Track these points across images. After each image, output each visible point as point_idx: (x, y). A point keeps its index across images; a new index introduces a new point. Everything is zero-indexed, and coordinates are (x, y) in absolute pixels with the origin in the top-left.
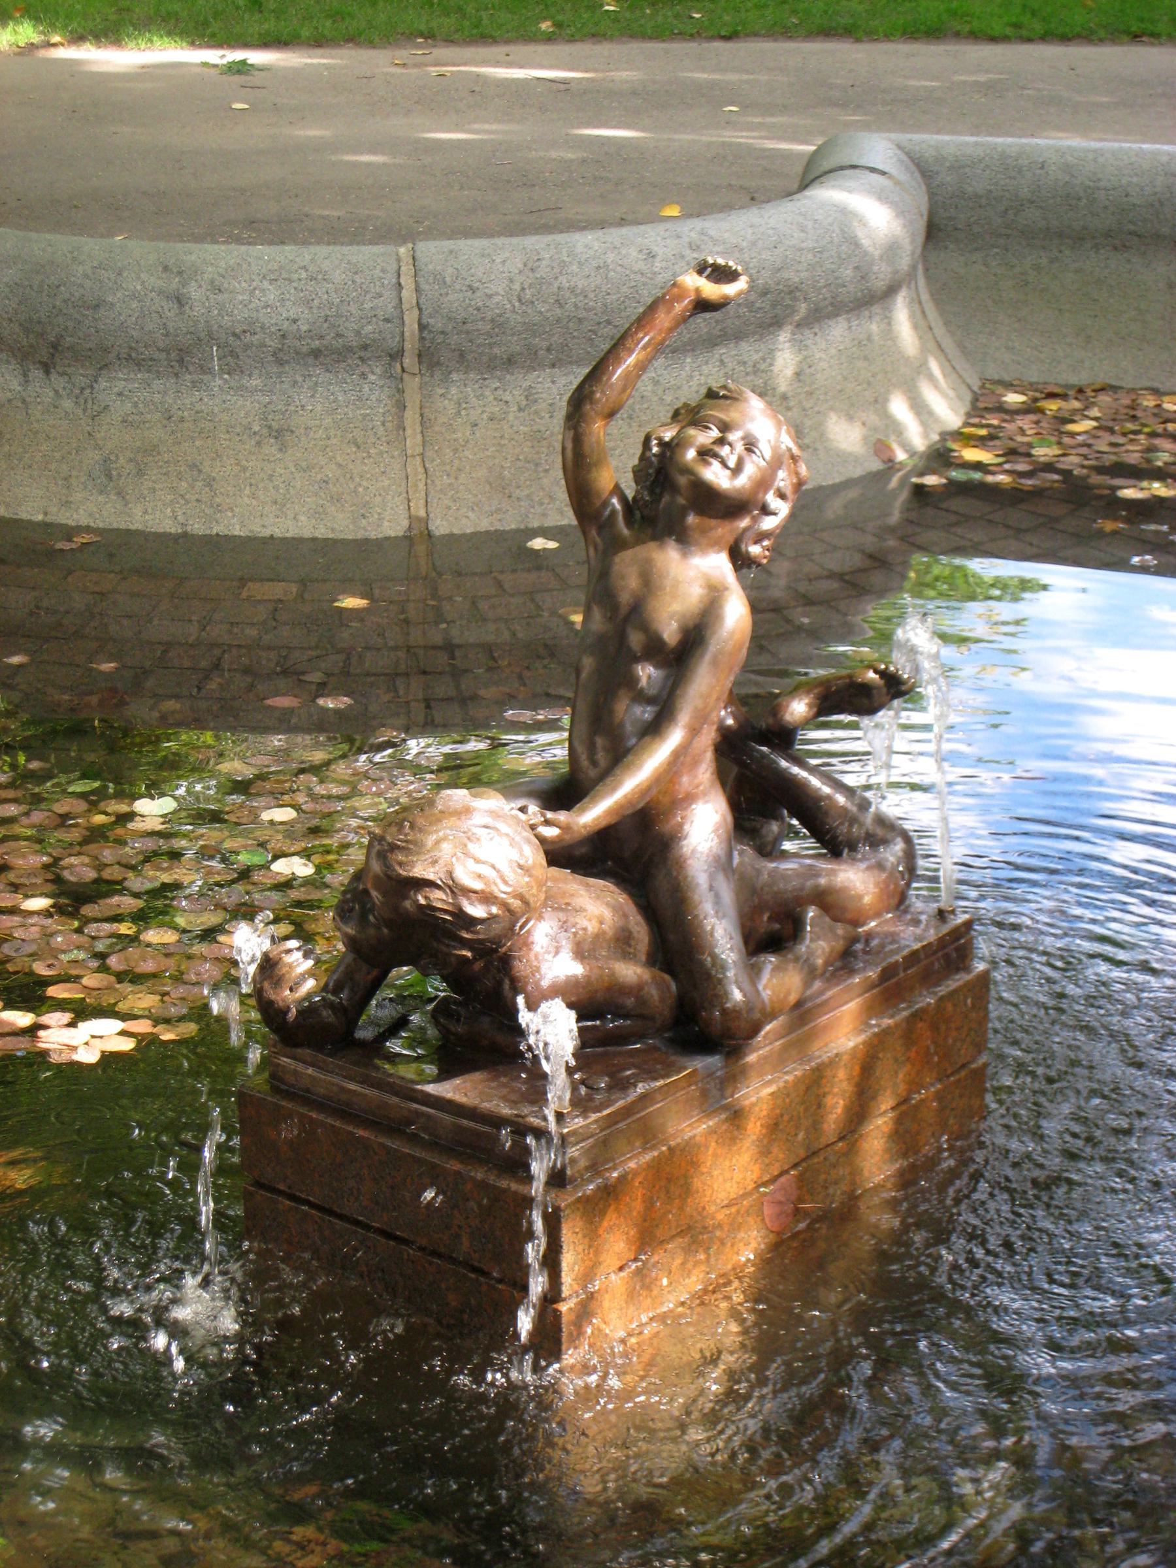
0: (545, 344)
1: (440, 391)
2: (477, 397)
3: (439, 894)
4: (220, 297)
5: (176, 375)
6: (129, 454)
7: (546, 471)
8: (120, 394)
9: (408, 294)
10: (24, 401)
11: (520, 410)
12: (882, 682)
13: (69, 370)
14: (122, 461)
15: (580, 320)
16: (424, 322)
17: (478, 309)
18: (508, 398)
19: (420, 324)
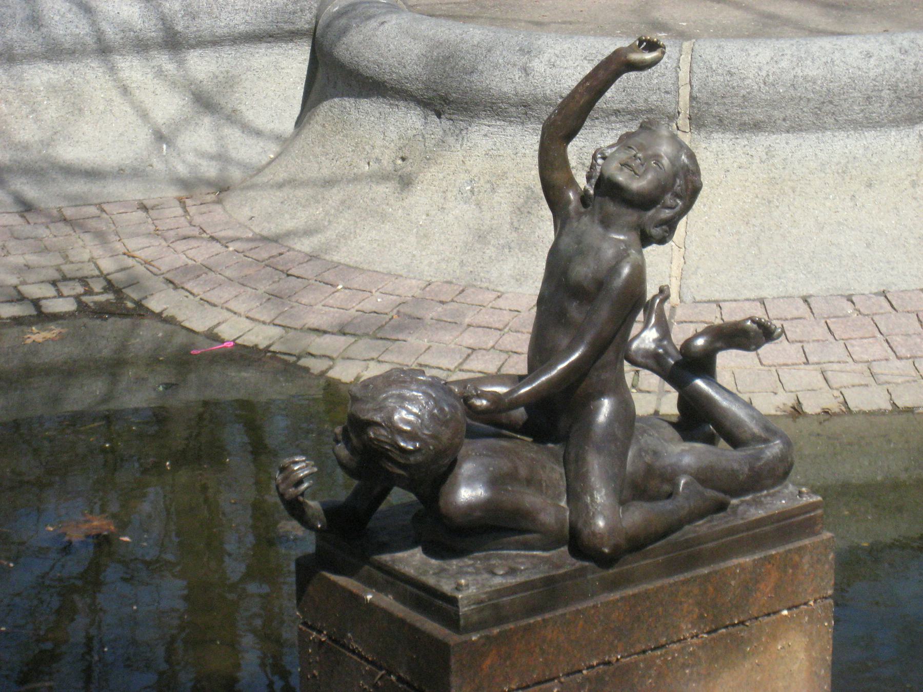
0: (782, 116)
1: (704, 145)
2: (731, 151)
3: (383, 432)
4: (554, 71)
5: (523, 123)
6: (487, 177)
7: (777, 207)
8: (485, 135)
9: (684, 74)
10: (423, 137)
11: (761, 162)
12: (761, 331)
13: (453, 117)
14: (482, 181)
15: (809, 100)
16: (694, 95)
17: (733, 88)
18: (754, 153)
19: (691, 97)
